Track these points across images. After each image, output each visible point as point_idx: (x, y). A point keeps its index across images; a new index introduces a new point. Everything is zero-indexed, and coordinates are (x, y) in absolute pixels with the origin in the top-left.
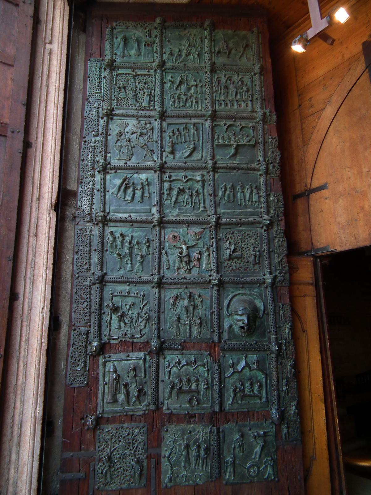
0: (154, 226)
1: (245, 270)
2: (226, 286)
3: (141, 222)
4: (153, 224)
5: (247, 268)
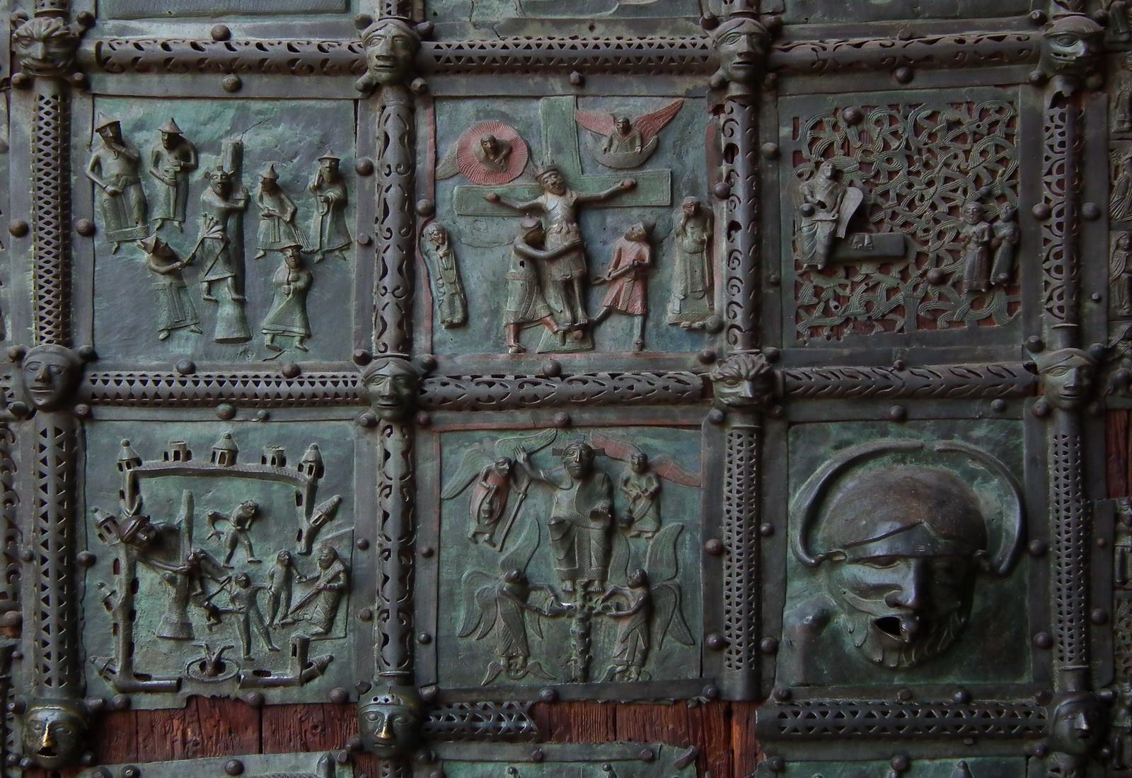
0: (371, 90)
1: (920, 322)
3: (292, 66)
4: (361, 80)
5: (936, 313)
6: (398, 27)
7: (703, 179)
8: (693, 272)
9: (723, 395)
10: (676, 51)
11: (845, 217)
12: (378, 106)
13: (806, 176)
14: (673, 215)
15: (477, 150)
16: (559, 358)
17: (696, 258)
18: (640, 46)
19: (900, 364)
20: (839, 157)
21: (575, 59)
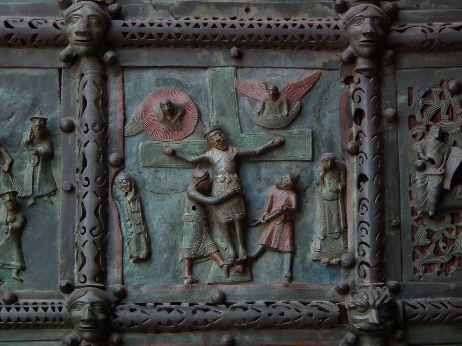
4: (64, 52)
6: (93, 8)
7: (337, 139)
8: (331, 216)
9: (356, 321)
10: (315, 31)
11: (450, 172)
12: (78, 74)
13: (419, 137)
14: (314, 168)
15: (157, 111)
16: (225, 288)
17: (333, 204)
18: (286, 26)
20: (445, 122)
21: (234, 36)
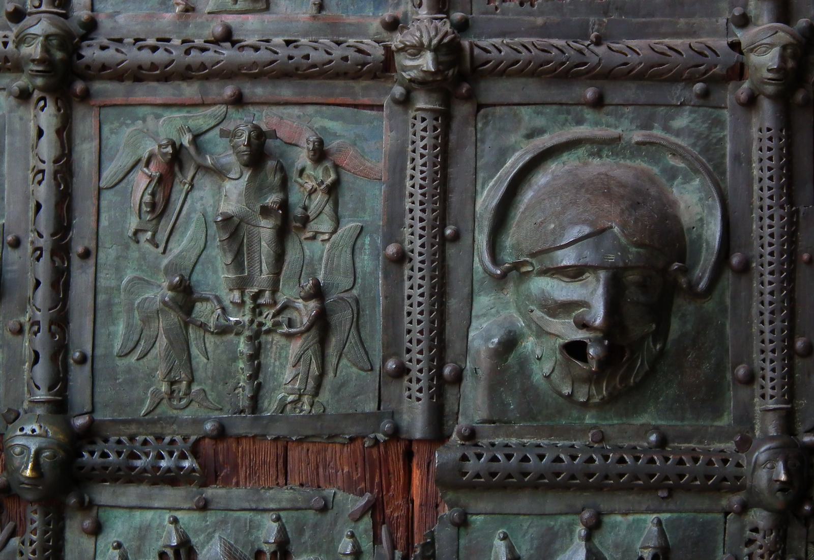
2: (495, 90)
9: (405, 69)
16: (230, 19)
19: (597, 37)
